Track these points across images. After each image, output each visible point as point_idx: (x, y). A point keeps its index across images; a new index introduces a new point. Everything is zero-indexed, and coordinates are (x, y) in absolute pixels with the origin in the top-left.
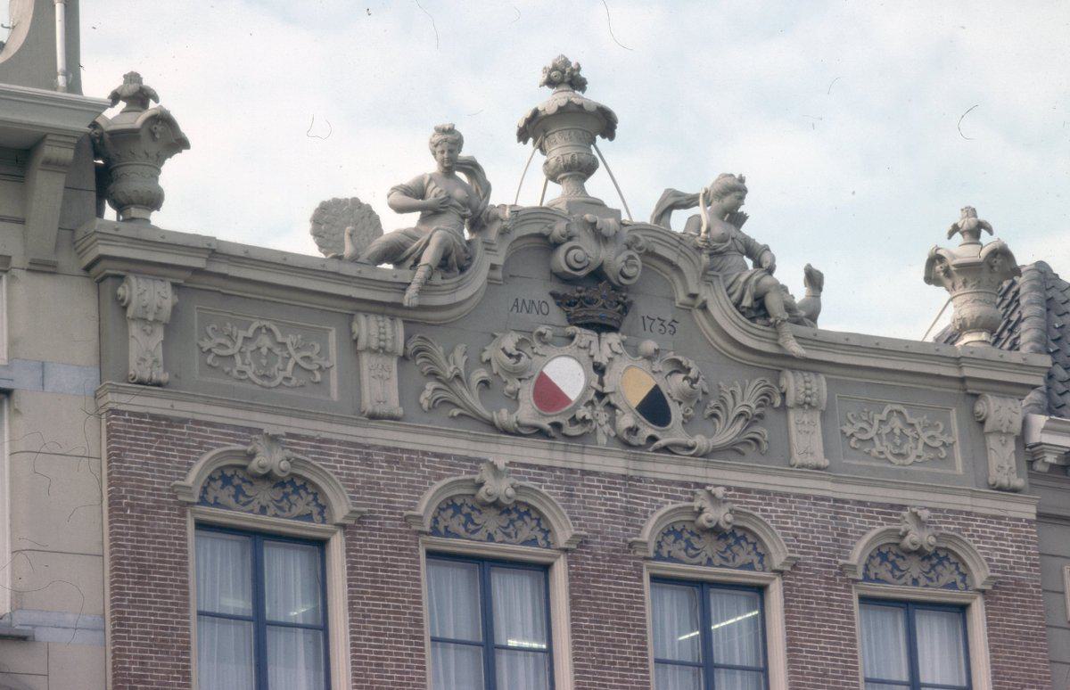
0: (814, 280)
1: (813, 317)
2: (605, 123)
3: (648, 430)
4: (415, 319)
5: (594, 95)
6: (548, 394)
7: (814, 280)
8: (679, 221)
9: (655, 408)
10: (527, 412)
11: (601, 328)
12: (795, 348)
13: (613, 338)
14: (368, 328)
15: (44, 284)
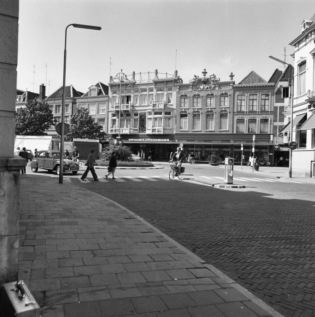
0: (219, 79)
1: (220, 81)
2: (207, 73)
3: (207, 89)
4: (193, 86)
5: (206, 71)
6: (200, 88)
7: (219, 79)
8: (211, 77)
9: (207, 88)
10: (199, 90)
11: (204, 84)
12: (216, 83)
13: (205, 85)
14: (190, 87)
15: (174, 87)
